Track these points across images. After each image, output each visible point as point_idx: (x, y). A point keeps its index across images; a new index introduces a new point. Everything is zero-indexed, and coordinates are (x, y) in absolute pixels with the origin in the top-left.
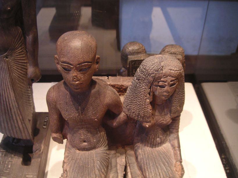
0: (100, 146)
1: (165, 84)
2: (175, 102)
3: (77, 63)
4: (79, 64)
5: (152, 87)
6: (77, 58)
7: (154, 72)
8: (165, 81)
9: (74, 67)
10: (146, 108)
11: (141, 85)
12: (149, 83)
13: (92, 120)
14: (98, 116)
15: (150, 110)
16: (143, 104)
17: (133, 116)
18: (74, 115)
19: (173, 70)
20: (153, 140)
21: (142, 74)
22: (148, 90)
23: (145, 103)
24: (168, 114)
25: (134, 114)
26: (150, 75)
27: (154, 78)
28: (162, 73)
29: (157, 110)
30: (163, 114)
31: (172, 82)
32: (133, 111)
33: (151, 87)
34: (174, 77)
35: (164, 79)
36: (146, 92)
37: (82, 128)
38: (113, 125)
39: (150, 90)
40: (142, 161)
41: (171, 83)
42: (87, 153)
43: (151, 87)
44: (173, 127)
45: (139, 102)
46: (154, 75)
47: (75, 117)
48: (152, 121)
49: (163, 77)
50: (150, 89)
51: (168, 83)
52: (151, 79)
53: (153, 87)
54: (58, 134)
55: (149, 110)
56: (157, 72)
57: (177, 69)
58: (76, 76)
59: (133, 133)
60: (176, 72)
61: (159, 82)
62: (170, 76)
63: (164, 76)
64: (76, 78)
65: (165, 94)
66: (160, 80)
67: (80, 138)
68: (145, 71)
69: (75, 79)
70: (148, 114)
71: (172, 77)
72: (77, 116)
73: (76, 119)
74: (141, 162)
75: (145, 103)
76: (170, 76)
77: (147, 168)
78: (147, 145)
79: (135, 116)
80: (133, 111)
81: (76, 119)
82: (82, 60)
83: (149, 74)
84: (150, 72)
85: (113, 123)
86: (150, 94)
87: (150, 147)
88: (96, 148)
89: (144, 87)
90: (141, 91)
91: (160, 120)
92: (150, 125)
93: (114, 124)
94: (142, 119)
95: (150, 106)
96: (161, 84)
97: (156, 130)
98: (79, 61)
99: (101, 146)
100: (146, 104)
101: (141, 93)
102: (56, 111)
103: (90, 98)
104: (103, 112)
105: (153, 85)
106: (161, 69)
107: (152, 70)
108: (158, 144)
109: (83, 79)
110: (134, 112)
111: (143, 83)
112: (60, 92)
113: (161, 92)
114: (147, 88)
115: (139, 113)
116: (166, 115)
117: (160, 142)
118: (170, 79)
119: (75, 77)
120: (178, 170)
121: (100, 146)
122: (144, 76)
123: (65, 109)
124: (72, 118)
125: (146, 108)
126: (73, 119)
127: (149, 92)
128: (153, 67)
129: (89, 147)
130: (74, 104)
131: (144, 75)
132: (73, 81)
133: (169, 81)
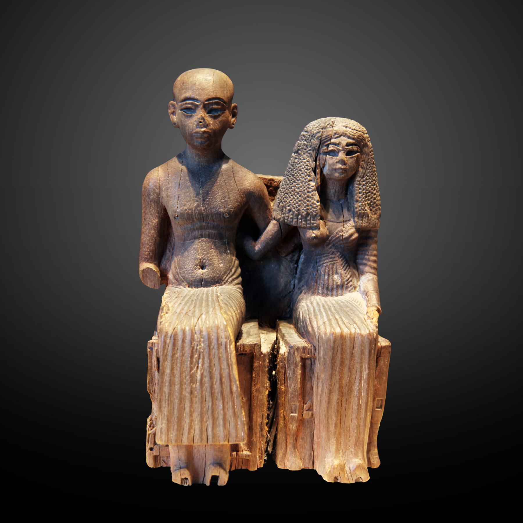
0: (229, 280)
1: (337, 149)
2: (360, 193)
3: (206, 97)
4: (209, 100)
5: (318, 158)
6: (206, 91)
7: (321, 130)
8: (338, 142)
9: (201, 104)
10: (311, 197)
11: (301, 157)
12: (313, 151)
13: (220, 215)
14: (230, 208)
15: (318, 202)
16: (304, 191)
17: (289, 219)
18: (191, 204)
19: (350, 128)
20: (326, 277)
21: (302, 141)
22: (312, 164)
23: (309, 188)
24: (350, 220)
25: (291, 213)
26: (314, 137)
27: (320, 138)
28: (332, 131)
29: (331, 210)
30: (341, 219)
31: (350, 147)
32: (289, 208)
33: (316, 158)
34: (353, 139)
35: (335, 140)
36: (309, 168)
37: (202, 236)
38: (255, 250)
39: (314, 163)
40: (307, 312)
41: (346, 147)
42: (205, 290)
43: (316, 158)
44: (364, 262)
45: (298, 188)
46: (319, 134)
47: (192, 209)
48: (321, 229)
49: (334, 135)
50: (316, 161)
51: (344, 149)
52: (315, 142)
53: (319, 157)
54: (153, 264)
55: (315, 202)
56: (324, 129)
57: (357, 129)
58: (203, 119)
59: (292, 287)
60: (355, 131)
61: (328, 146)
62: (344, 136)
63: (335, 134)
64: (202, 121)
65: (339, 166)
66: (329, 142)
67: (195, 259)
68: (307, 133)
69: (201, 124)
70: (315, 210)
71: (349, 137)
72: (196, 207)
73: (192, 212)
74: (304, 315)
75: (309, 188)
76: (344, 135)
77: (315, 315)
78: (316, 291)
79: (292, 218)
80: (289, 208)
81: (192, 212)
82: (213, 95)
83: (312, 136)
84: (315, 132)
85: (254, 246)
86: (315, 171)
87: (323, 294)
88: (223, 283)
89: (305, 161)
90: (301, 167)
91: (336, 231)
92: (319, 234)
93: (257, 248)
94: (304, 222)
95: (317, 194)
96: (331, 148)
97: (331, 256)
98: (209, 95)
99: (231, 282)
100: (310, 190)
101: (301, 171)
102: (158, 208)
103: (218, 175)
104: (238, 203)
105: (320, 154)
106: (331, 125)
107: (317, 128)
108: (338, 286)
109: (212, 125)
110: (290, 210)
111: (304, 154)
112: (169, 169)
113: (333, 164)
114: (310, 161)
115: (299, 210)
116: (346, 221)
117: (339, 282)
118: (345, 141)
119: (201, 119)
120: (371, 316)
121: (229, 280)
122: (305, 143)
123: (175, 196)
124: (186, 210)
125: (311, 197)
126: (188, 211)
127: (313, 166)
128: (319, 124)
129: (210, 277)
130: (193, 186)
131: (305, 140)
132: (197, 128)
133: (344, 143)
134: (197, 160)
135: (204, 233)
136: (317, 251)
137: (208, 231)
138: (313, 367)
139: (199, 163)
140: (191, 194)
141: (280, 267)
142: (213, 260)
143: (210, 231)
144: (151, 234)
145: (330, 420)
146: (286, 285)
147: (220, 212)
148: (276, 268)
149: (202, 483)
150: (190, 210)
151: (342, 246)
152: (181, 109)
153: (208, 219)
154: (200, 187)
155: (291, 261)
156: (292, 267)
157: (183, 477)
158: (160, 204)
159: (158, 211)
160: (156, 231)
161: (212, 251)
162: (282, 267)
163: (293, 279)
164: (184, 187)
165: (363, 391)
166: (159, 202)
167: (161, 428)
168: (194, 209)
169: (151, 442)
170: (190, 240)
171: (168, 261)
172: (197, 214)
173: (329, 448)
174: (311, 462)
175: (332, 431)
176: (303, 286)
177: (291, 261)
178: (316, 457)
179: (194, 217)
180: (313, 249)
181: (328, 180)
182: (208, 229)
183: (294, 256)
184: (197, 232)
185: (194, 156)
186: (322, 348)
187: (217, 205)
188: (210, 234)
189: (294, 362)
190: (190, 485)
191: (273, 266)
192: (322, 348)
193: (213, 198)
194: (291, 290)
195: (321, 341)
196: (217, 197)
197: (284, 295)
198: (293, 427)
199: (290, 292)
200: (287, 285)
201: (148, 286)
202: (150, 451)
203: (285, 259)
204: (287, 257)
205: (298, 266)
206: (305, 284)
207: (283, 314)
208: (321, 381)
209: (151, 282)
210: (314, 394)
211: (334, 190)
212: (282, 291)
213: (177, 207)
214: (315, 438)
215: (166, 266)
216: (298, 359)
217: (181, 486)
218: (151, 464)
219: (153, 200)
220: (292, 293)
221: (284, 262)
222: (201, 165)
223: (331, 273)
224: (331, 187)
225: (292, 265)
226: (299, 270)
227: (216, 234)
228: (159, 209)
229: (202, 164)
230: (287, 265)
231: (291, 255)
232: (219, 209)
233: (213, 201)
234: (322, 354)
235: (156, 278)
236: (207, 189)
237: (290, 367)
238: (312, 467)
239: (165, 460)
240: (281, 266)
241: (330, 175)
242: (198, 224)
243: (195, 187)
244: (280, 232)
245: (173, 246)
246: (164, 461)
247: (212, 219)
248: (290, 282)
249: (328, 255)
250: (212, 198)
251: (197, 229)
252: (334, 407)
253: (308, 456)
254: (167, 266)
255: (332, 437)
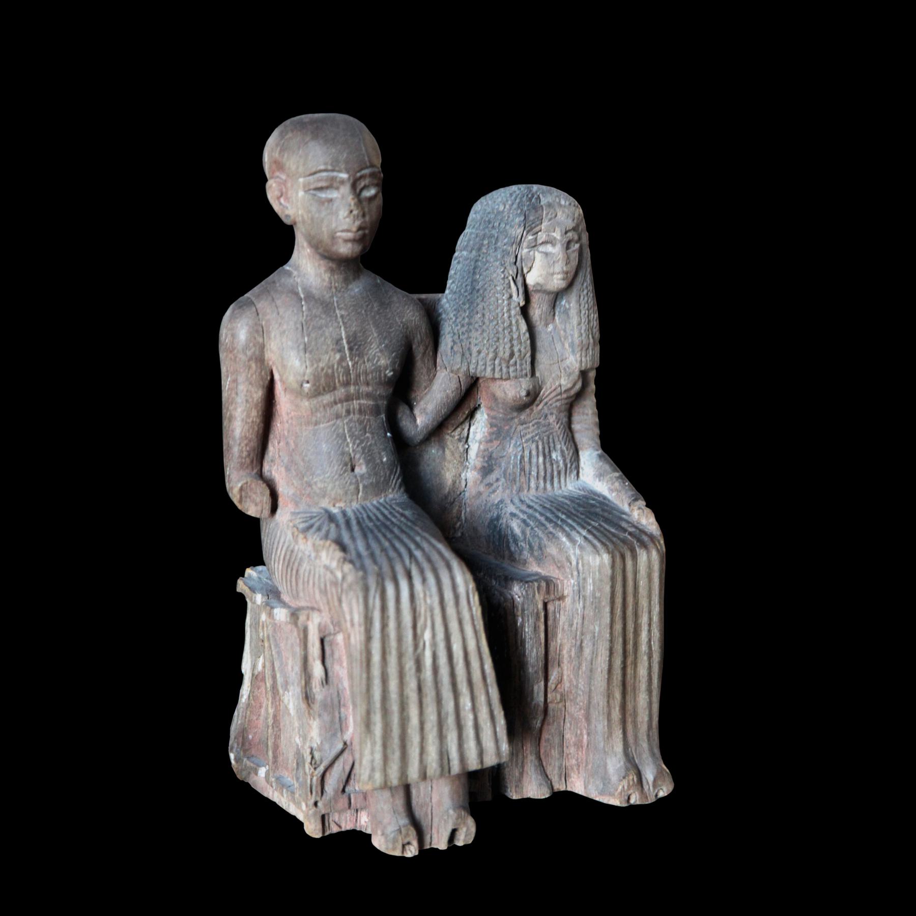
53: (521, 256)
73: (333, 372)
81: (333, 372)
124: (323, 369)
134: (327, 279)
135: (352, 407)
136: (522, 417)
137: (358, 402)
138: (558, 616)
139: (331, 283)
140: (327, 340)
141: (444, 451)
142: (372, 454)
143: (362, 402)
144: (251, 419)
145: (611, 701)
146: (454, 482)
147: (380, 366)
148: (439, 454)
149: (428, 847)
150: (329, 368)
151: (558, 404)
152: (306, 189)
153: (358, 381)
154: (341, 327)
155: (460, 440)
156: (461, 449)
157: (406, 841)
158: (266, 363)
159: (262, 376)
160: (260, 413)
161: (368, 437)
162: (447, 452)
163: (463, 470)
164: (312, 330)
165: (654, 643)
166: (264, 360)
167: (373, 761)
168: (336, 367)
169: (317, 792)
170: (328, 421)
171: (274, 465)
172: (341, 375)
173: (613, 748)
174: (563, 779)
175: (616, 719)
176: (497, 480)
177: (460, 440)
178: (572, 769)
179: (337, 381)
180: (515, 414)
181: (533, 293)
182: (358, 398)
183: (463, 429)
184: (339, 405)
185: (323, 272)
186: (590, 581)
187: (375, 355)
188: (362, 408)
189: (535, 611)
190: (417, 854)
191: (433, 451)
192: (590, 581)
193: (365, 344)
194: (462, 490)
195: (586, 568)
196: (372, 340)
197: (452, 500)
198: (536, 723)
199: (460, 494)
200: (455, 482)
201: (249, 513)
202: (315, 808)
203: (451, 436)
204: (453, 434)
205: (469, 446)
206: (503, 475)
207: (451, 533)
208: (588, 637)
209: (256, 505)
210: (565, 661)
211: (540, 310)
212: (449, 492)
213: (306, 367)
214: (568, 736)
215: (271, 473)
216: (540, 606)
217: (403, 858)
218: (317, 832)
219: (254, 358)
220: (463, 494)
221: (449, 443)
222: (336, 288)
223: (547, 450)
224: (535, 306)
225: (460, 445)
226: (473, 453)
227: (371, 407)
228: (263, 373)
229: (337, 285)
230: (454, 447)
231: (459, 429)
232: (378, 361)
233: (365, 348)
234: (589, 591)
235: (265, 498)
236: (354, 329)
237: (528, 620)
238: (565, 787)
239: (337, 820)
240: (446, 449)
241: (542, 286)
242: (341, 392)
243: (332, 325)
244: (459, 391)
245: (278, 436)
246: (335, 822)
247: (366, 379)
248: (460, 476)
249: (539, 421)
250: (363, 343)
251: (341, 401)
252: (617, 678)
253: (557, 768)
254: (273, 473)
255: (616, 729)
